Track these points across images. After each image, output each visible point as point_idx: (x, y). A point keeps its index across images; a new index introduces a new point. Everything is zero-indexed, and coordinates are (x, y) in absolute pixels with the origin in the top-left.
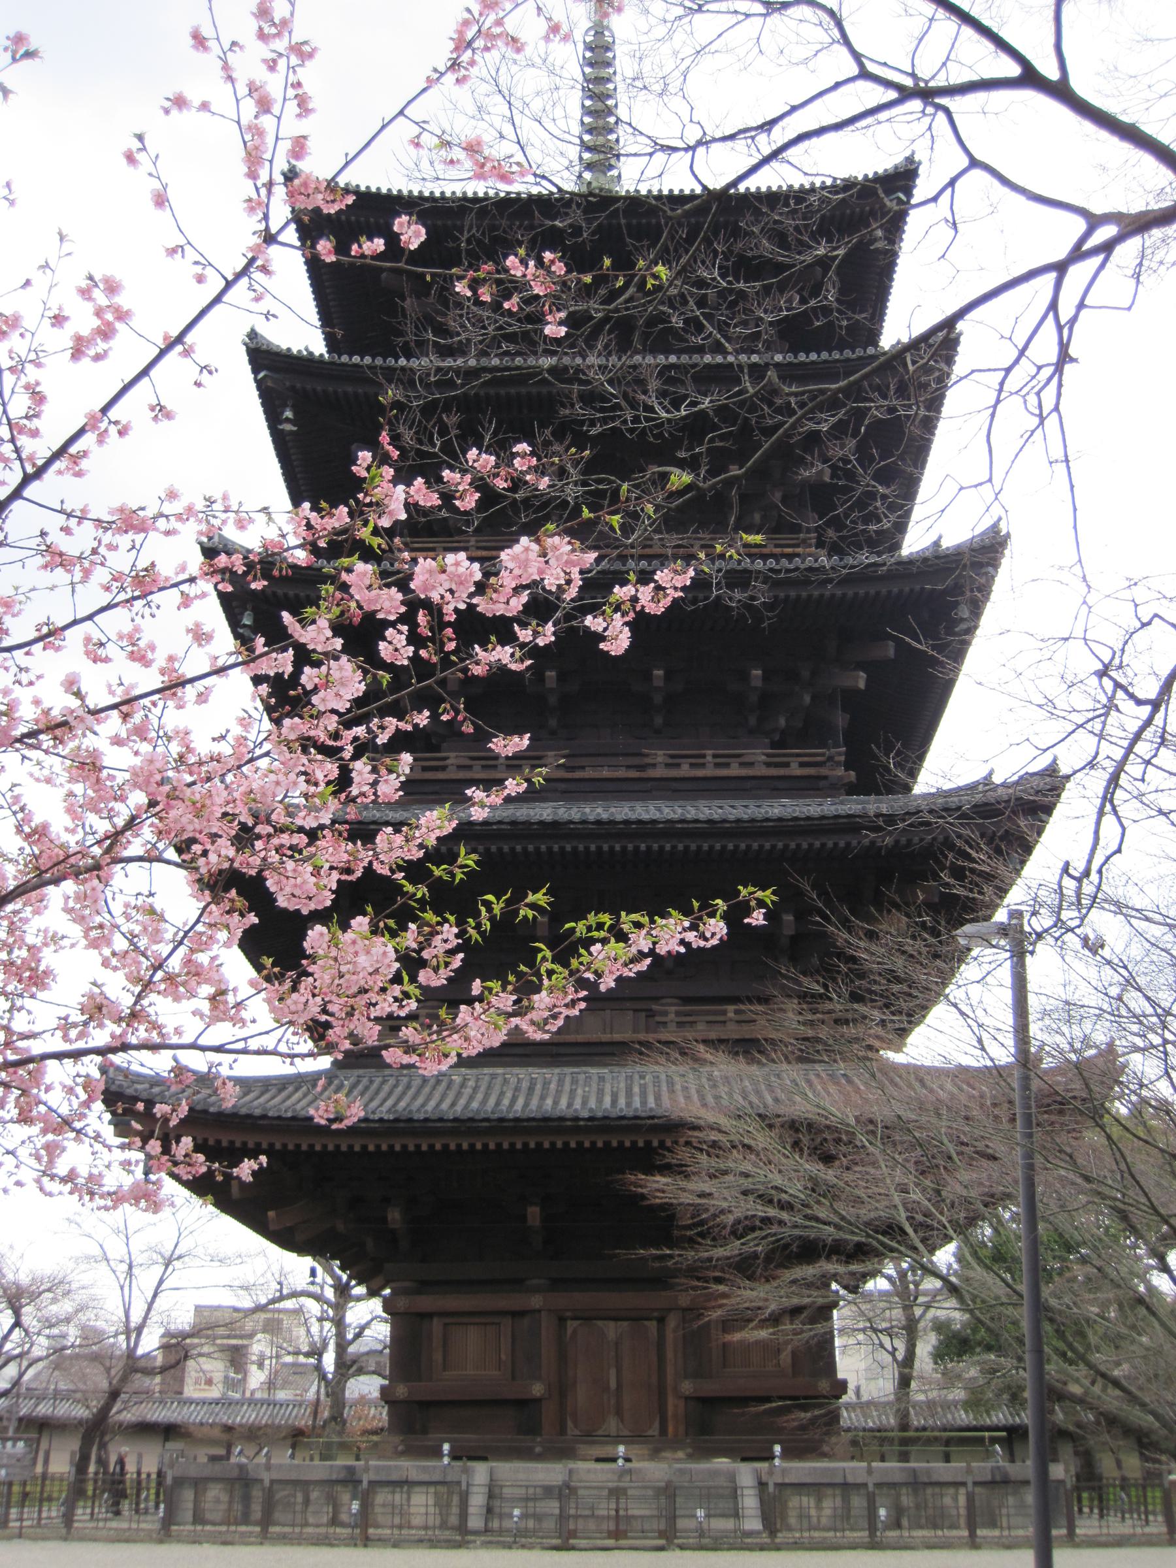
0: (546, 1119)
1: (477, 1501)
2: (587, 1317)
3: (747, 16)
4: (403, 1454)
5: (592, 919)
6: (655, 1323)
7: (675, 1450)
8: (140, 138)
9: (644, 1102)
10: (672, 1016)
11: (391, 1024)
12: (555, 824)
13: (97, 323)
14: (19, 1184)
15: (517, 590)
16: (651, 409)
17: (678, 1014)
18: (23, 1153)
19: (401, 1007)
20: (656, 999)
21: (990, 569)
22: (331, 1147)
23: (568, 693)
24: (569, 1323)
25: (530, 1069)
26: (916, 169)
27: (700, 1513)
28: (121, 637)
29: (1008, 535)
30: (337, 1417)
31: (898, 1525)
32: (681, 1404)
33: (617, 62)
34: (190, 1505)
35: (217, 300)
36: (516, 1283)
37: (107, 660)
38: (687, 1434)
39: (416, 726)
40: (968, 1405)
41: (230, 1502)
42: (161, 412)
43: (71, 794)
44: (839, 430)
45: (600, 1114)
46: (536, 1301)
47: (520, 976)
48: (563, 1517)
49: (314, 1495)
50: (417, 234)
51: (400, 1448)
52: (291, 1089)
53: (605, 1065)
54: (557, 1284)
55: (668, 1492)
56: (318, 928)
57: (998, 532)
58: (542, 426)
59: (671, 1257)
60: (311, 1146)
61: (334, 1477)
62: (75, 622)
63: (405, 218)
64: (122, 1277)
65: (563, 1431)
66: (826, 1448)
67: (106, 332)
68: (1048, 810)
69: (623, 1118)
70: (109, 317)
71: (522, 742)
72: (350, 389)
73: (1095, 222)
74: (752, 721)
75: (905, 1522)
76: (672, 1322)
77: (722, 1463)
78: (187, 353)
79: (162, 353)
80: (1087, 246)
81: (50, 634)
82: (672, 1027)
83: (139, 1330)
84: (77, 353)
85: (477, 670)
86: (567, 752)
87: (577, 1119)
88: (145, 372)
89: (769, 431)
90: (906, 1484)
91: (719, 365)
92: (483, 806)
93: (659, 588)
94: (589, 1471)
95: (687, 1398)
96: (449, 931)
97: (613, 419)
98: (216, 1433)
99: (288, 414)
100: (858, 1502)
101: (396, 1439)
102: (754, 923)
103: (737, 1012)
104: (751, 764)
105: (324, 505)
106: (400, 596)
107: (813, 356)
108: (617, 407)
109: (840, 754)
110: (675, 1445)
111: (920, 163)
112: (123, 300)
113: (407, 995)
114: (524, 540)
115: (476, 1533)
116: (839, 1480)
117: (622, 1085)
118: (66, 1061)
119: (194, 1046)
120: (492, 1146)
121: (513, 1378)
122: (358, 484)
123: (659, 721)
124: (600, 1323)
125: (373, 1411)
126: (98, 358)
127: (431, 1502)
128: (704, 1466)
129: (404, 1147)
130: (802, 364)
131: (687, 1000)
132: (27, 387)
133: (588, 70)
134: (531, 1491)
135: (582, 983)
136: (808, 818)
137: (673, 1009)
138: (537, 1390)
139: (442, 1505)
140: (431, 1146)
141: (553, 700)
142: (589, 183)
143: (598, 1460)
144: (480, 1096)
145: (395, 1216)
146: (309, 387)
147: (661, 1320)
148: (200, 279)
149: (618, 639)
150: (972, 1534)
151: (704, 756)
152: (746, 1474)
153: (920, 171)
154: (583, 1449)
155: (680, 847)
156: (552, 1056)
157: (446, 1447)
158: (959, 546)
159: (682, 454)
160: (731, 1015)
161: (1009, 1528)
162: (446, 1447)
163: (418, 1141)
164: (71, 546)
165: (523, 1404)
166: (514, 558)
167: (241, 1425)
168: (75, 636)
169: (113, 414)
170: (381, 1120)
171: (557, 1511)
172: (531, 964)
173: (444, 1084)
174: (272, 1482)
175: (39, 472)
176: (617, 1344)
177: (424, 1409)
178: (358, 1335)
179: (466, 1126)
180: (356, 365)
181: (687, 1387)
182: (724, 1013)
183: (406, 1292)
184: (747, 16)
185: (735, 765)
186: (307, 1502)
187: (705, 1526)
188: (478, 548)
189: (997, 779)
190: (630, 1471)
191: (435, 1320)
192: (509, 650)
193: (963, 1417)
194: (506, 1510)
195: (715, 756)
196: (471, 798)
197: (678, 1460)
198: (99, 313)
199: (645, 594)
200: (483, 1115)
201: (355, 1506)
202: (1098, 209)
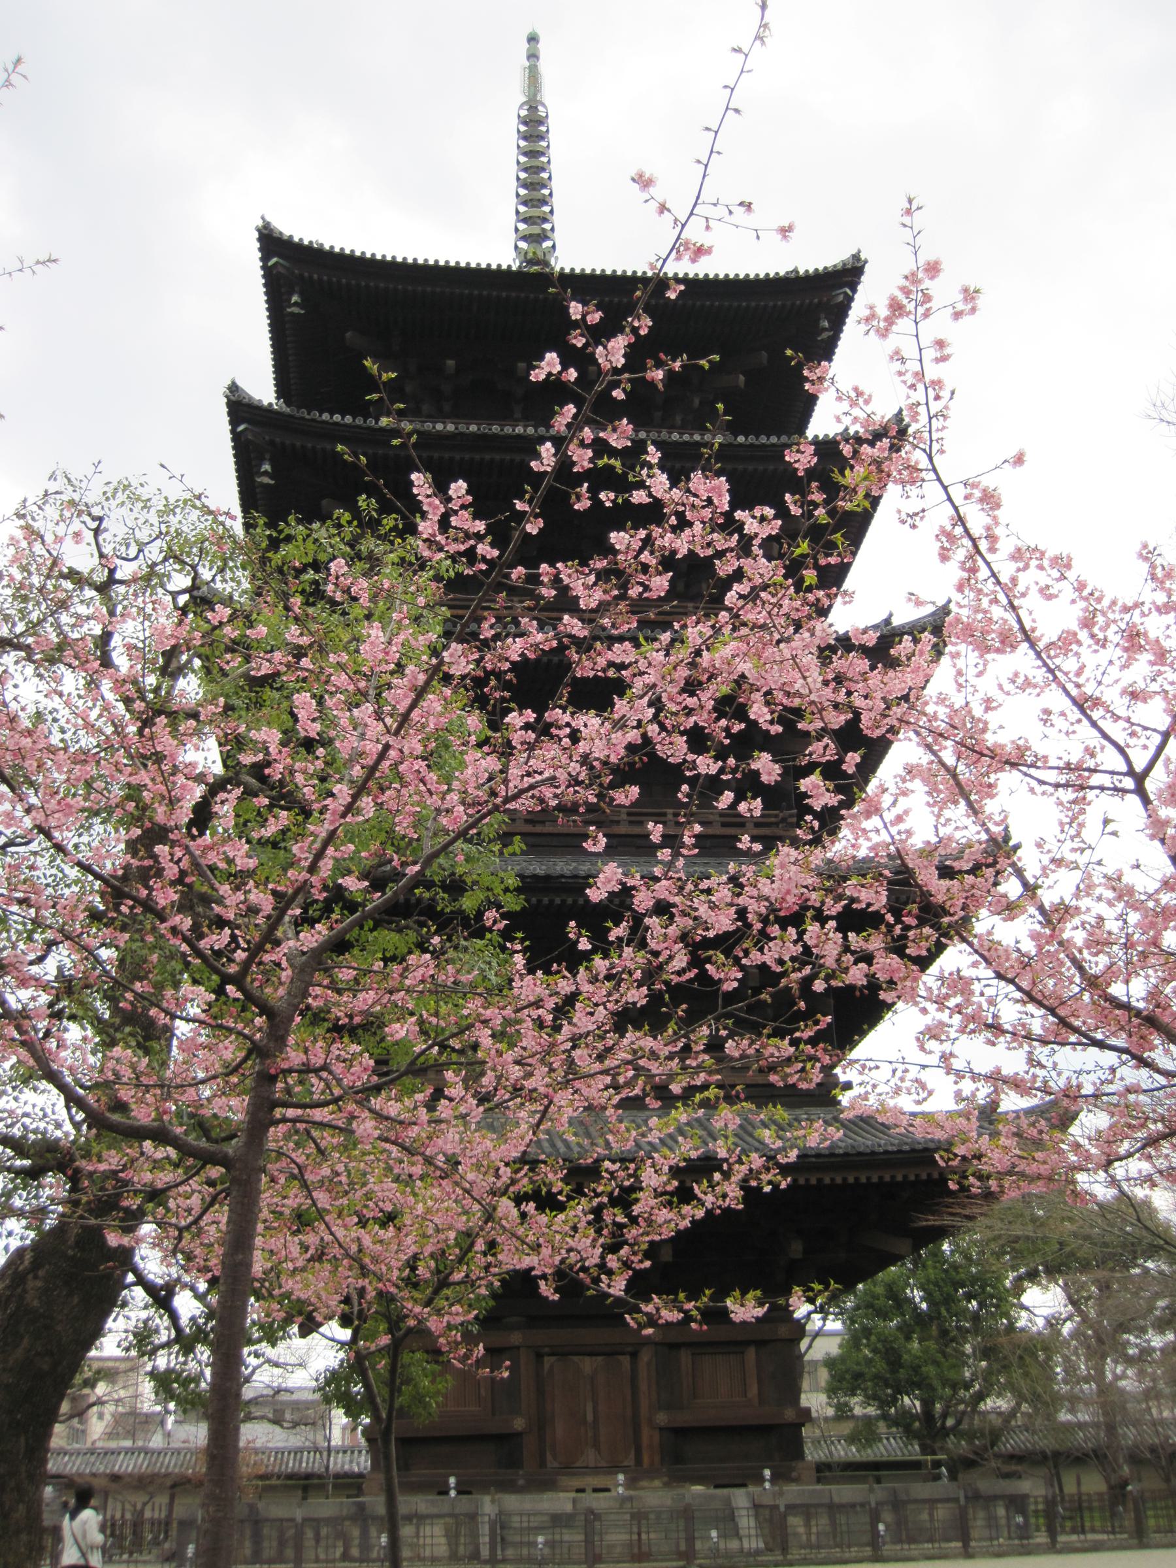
2: (562, 1353)
7: (652, 1479)
12: (548, 878)
24: (546, 1359)
27: (714, 1533)
40: (852, 1439)
48: (589, 1542)
49: (324, 1531)
61: (345, 1512)
65: (542, 1464)
66: (794, 1474)
76: (645, 1356)
77: (698, 1488)
91: (686, 443)
95: (661, 1429)
99: (267, 467)
109: (791, 816)
110: (651, 1474)
111: (866, 262)
116: (826, 1501)
124: (576, 1358)
134: (546, 1518)
138: (519, 1424)
139: (452, 1537)
146: (288, 442)
147: (634, 1355)
150: (966, 1546)
151: (665, 814)
152: (740, 1498)
153: (867, 268)
154: (565, 1481)
157: (452, 1481)
162: (452, 1481)
167: (130, 1475)
171: (582, 1537)
180: (336, 424)
181: (662, 1418)
187: (722, 1546)
190: (631, 1499)
193: (852, 1453)
194: (532, 1538)
197: (655, 1489)
201: (384, 1540)
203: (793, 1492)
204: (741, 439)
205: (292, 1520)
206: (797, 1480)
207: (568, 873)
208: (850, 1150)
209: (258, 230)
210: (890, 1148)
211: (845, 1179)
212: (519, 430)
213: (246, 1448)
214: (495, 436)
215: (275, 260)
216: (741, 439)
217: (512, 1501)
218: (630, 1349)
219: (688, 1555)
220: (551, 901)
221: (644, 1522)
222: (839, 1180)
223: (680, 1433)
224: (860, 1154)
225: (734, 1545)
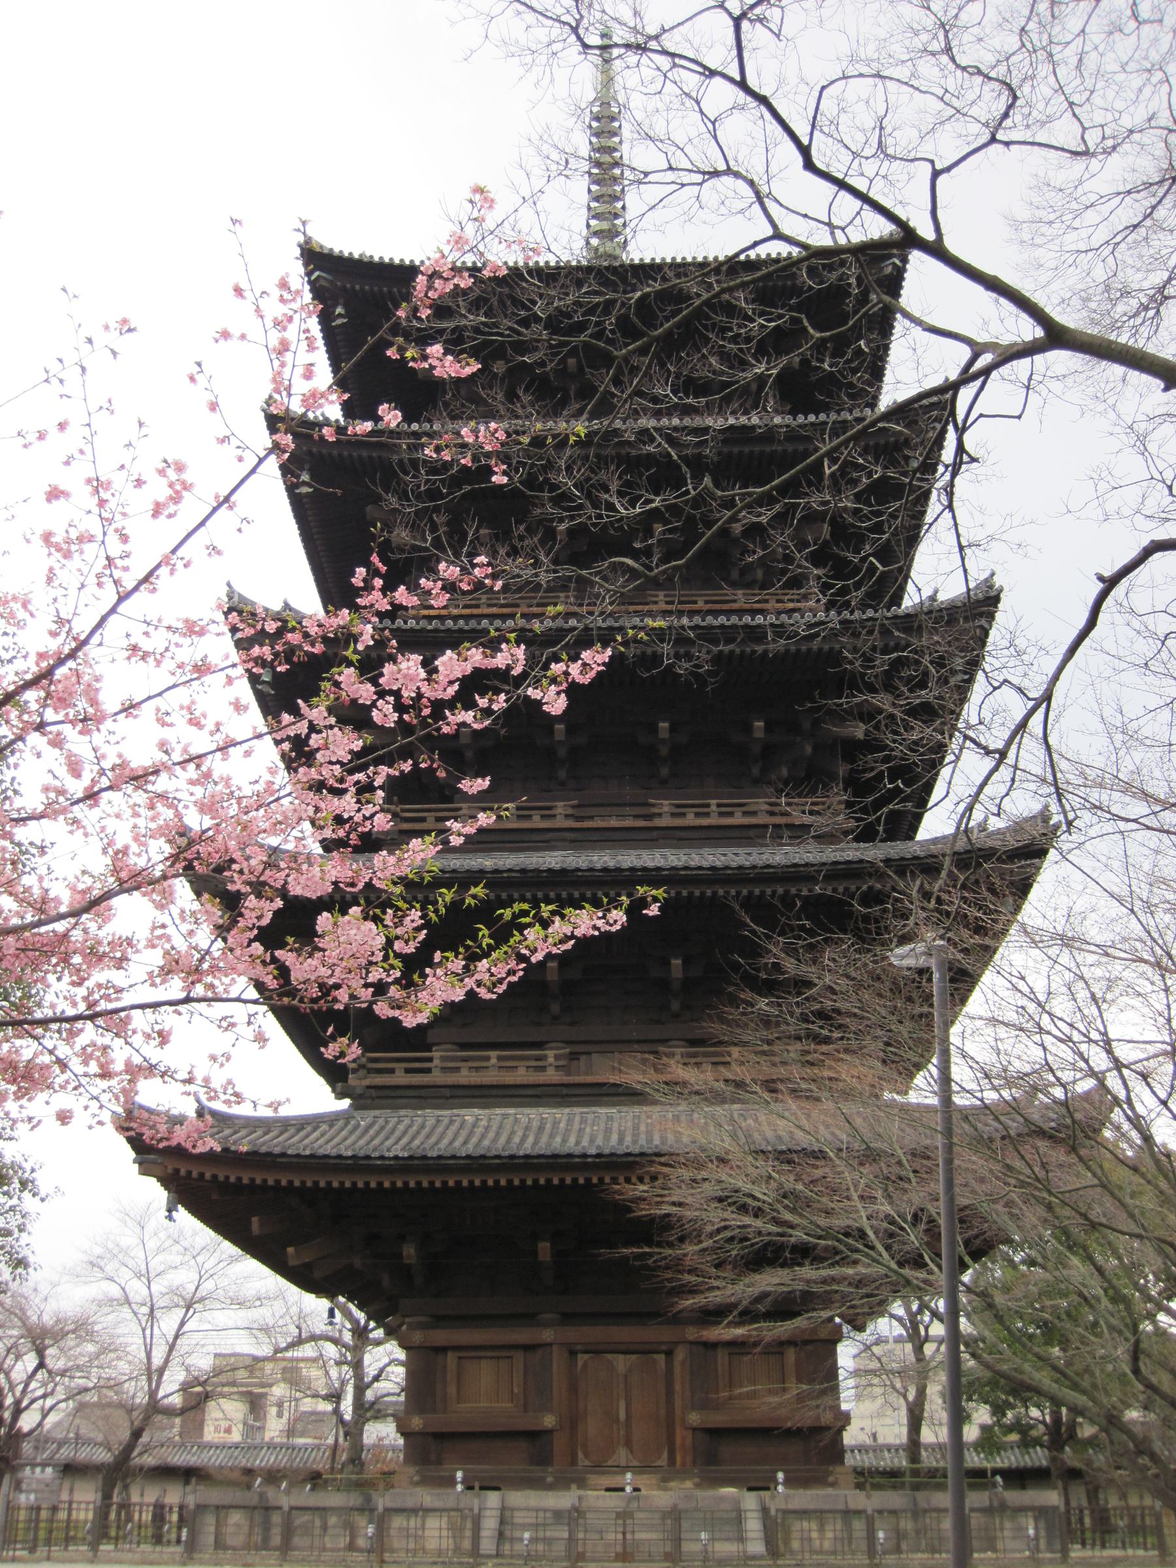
0: (555, 1156)
1: (490, 1524)
2: (596, 1351)
3: (683, 185)
4: (418, 1484)
5: (517, 907)
6: (663, 1356)
7: (684, 1480)
8: (199, 364)
9: (650, 1140)
11: (380, 988)
12: (563, 871)
13: (171, 492)
14: (100, 1123)
15: (451, 683)
16: (611, 507)
18: (105, 1098)
19: (389, 976)
20: (663, 1041)
21: (983, 622)
22: (348, 1184)
23: (517, 749)
24: (580, 1356)
25: (541, 1110)
27: (703, 1535)
28: (182, 708)
29: (1001, 590)
30: (356, 1460)
31: (898, 1550)
32: (689, 1434)
34: (212, 1529)
35: (253, 471)
36: (528, 1318)
37: (171, 725)
38: (694, 1463)
39: (402, 772)
41: (251, 1527)
42: (214, 550)
43: (135, 826)
44: (781, 519)
45: (607, 1151)
46: (548, 1335)
47: (467, 948)
48: (571, 1540)
49: (333, 1520)
50: (396, 417)
51: (416, 1478)
52: (309, 1129)
53: (614, 1105)
54: (568, 1318)
55: (675, 1515)
56: (325, 914)
57: (991, 587)
58: (518, 522)
59: (651, 1255)
60: (329, 1183)
61: (351, 1504)
62: (149, 698)
63: (386, 406)
64: (144, 1320)
65: (574, 1462)
66: (831, 1479)
67: (176, 499)
70: (178, 487)
71: (483, 783)
72: (365, 454)
73: (978, 350)
74: (756, 771)
75: (904, 1547)
76: (680, 1355)
78: (231, 508)
79: (215, 510)
80: (973, 369)
81: (132, 706)
83: (161, 1371)
84: (156, 513)
85: (446, 730)
86: (575, 802)
87: (585, 1156)
88: (202, 524)
89: (709, 524)
90: (905, 1511)
92: (459, 835)
93: (585, 665)
94: (598, 1497)
95: (694, 1429)
96: (415, 914)
97: (580, 516)
98: (236, 1475)
99: (305, 477)
100: (858, 1525)
101: (411, 1470)
102: (651, 914)
104: (754, 813)
105: (331, 608)
106: (373, 689)
108: (580, 507)
110: (682, 1474)
112: (187, 476)
113: (392, 967)
114: (449, 652)
115: (489, 1556)
116: (841, 1507)
117: (629, 1124)
118: (148, 1010)
119: (238, 999)
120: (503, 1183)
121: (525, 1411)
122: (357, 592)
123: (665, 771)
124: (609, 1356)
125: (390, 1454)
126: (170, 516)
127: (444, 1525)
128: (710, 1493)
129: (419, 1183)
132: (116, 531)
135: (521, 958)
137: (679, 1050)
138: (549, 1421)
139: (456, 1530)
140: (445, 1183)
141: (562, 752)
142: (597, 249)
143: (608, 1490)
144: (491, 1135)
145: (410, 1252)
147: (669, 1353)
148: (240, 459)
149: (556, 703)
151: (708, 806)
152: (750, 1501)
154: (593, 1479)
158: (953, 600)
159: (637, 545)
161: (1005, 1551)
163: (432, 1178)
164: (146, 645)
165: (533, 1435)
166: (444, 664)
168: (148, 709)
169: (179, 553)
170: (396, 1158)
171: (566, 1535)
172: (474, 938)
174: (292, 1508)
175: (128, 595)
176: (626, 1376)
177: (439, 1442)
178: (377, 1378)
181: (694, 1418)
183: (424, 1326)
184: (683, 185)
185: (738, 814)
186: (325, 1528)
187: (710, 1548)
188: (490, 606)
191: (450, 1354)
192: (471, 713)
194: (517, 1534)
195: (719, 805)
196: (449, 830)
198: (171, 485)
199: (575, 669)
201: (371, 1530)
202: (981, 338)
203: (804, 1498)
205: (280, 1508)
206: (833, 1485)
209: (300, 246)
213: (374, 1446)
215: (317, 274)
217: (519, 1498)
218: (664, 1347)
219: (674, 1556)
221: (629, 1521)
223: (716, 1433)
225: (726, 1548)
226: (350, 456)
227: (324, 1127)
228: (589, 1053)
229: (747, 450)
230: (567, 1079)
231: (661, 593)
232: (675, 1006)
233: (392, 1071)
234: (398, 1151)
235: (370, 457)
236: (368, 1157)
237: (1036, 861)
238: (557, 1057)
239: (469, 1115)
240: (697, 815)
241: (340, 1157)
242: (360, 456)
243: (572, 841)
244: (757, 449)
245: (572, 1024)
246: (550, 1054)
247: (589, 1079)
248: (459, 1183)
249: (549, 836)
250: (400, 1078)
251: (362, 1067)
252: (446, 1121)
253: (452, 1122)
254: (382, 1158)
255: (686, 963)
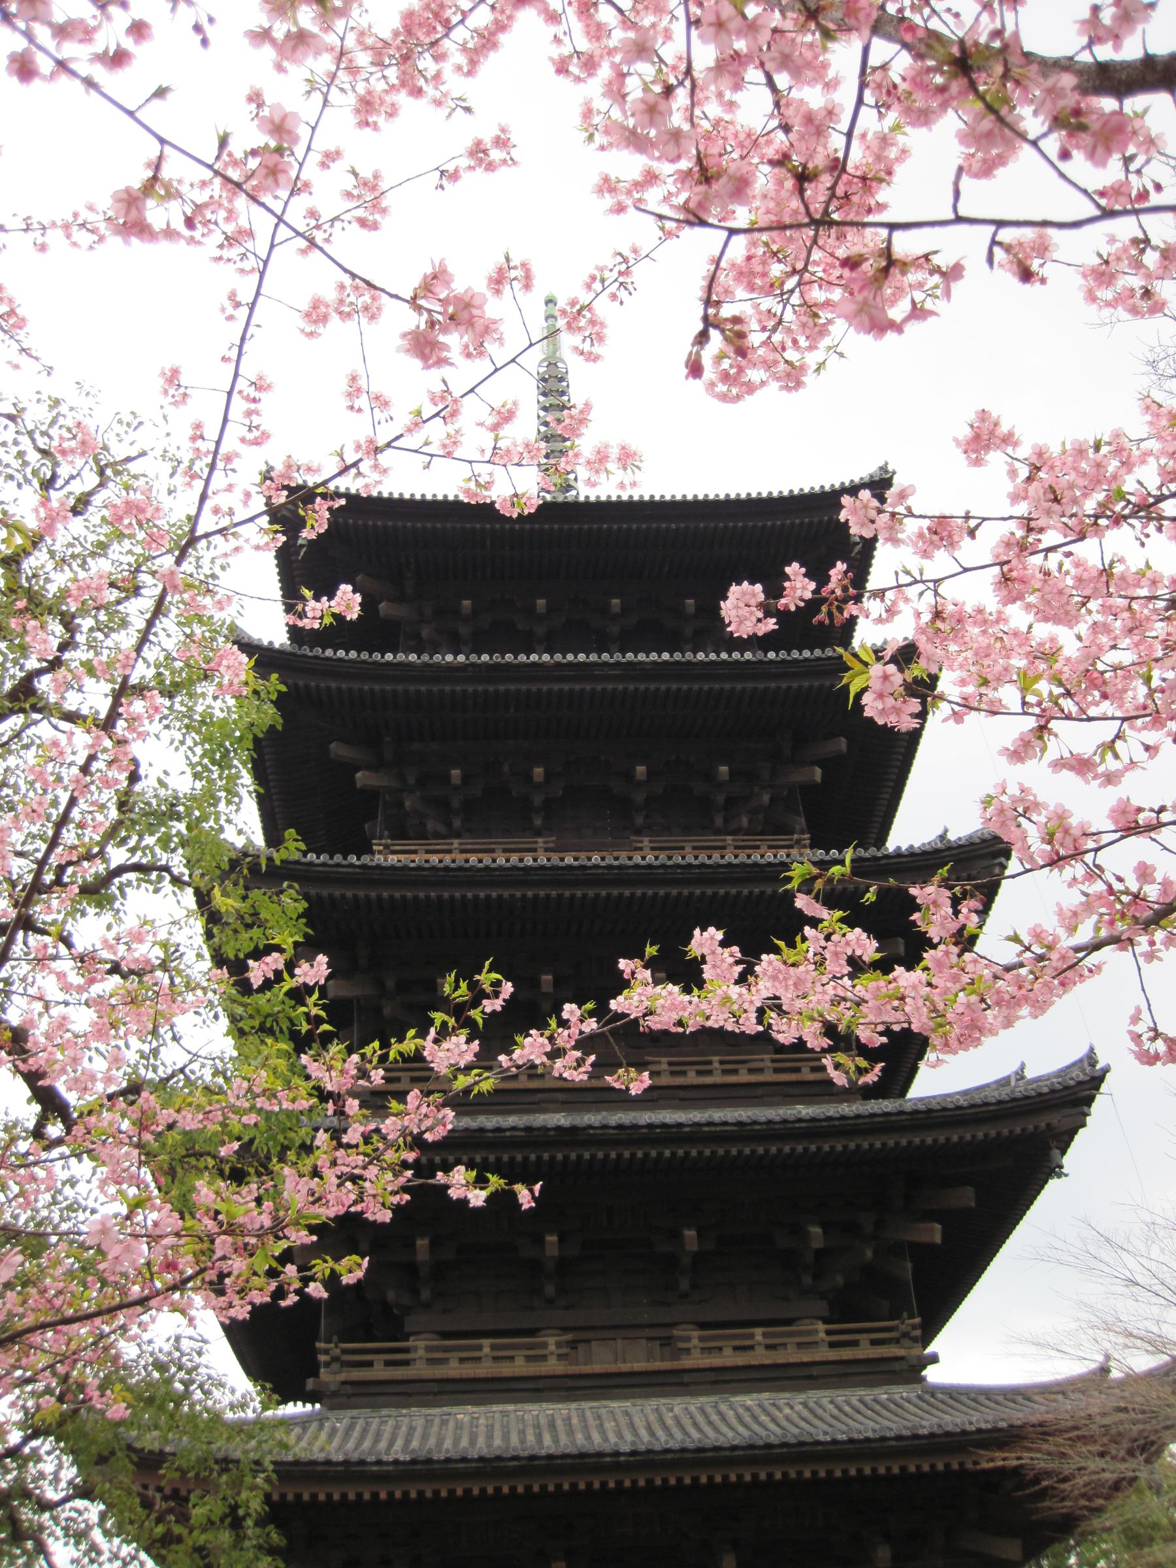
0: (582, 1455)
10: (695, 1342)
17: (701, 1339)
21: (1002, 860)
22: (336, 1497)
25: (544, 1405)
26: (891, 478)
33: (571, 391)
45: (642, 1448)
53: (626, 1397)
60: (314, 1496)
68: (1090, 1101)
69: (667, 1451)
72: (333, 685)
82: (696, 1353)
87: (617, 1454)
91: (712, 662)
103: (765, 1335)
104: (760, 1070)
107: (807, 654)
111: (894, 473)
129: (421, 1493)
130: (796, 661)
131: (703, 1326)
133: (542, 399)
136: (843, 1118)
140: (452, 1492)
151: (710, 1063)
155: (707, 1152)
156: (568, 1389)
158: (970, 837)
160: (759, 1338)
163: (436, 1487)
170: (396, 1462)
173: (451, 1425)
179: (491, 1466)
180: (341, 660)
182: (752, 1336)
189: (1030, 1074)
195: (722, 1062)
200: (511, 1453)
204: (771, 655)
207: (597, 1124)
208: (936, 1430)
210: (984, 1426)
211: (933, 1466)
212: (534, 657)
214: (508, 665)
216: (771, 655)
220: (580, 1157)
222: (926, 1468)
224: (948, 1434)
226: (318, 687)
227: (298, 1430)
228: (588, 1341)
229: (739, 686)
230: (573, 1369)
231: (646, 839)
232: (684, 1285)
233: (370, 1364)
234: (398, 1452)
235: (339, 689)
236: (362, 1462)
237: (1085, 1109)
238: (559, 1345)
239: (463, 1414)
240: (699, 1073)
241: (328, 1462)
242: (328, 689)
243: (563, 1103)
244: (750, 685)
245: (567, 1308)
246: (551, 1341)
247: (597, 1368)
248: (468, 1491)
249: (539, 1097)
250: (379, 1372)
251: (335, 1359)
252: (437, 1420)
253: (444, 1423)
254: (379, 1462)
255: (699, 1235)
